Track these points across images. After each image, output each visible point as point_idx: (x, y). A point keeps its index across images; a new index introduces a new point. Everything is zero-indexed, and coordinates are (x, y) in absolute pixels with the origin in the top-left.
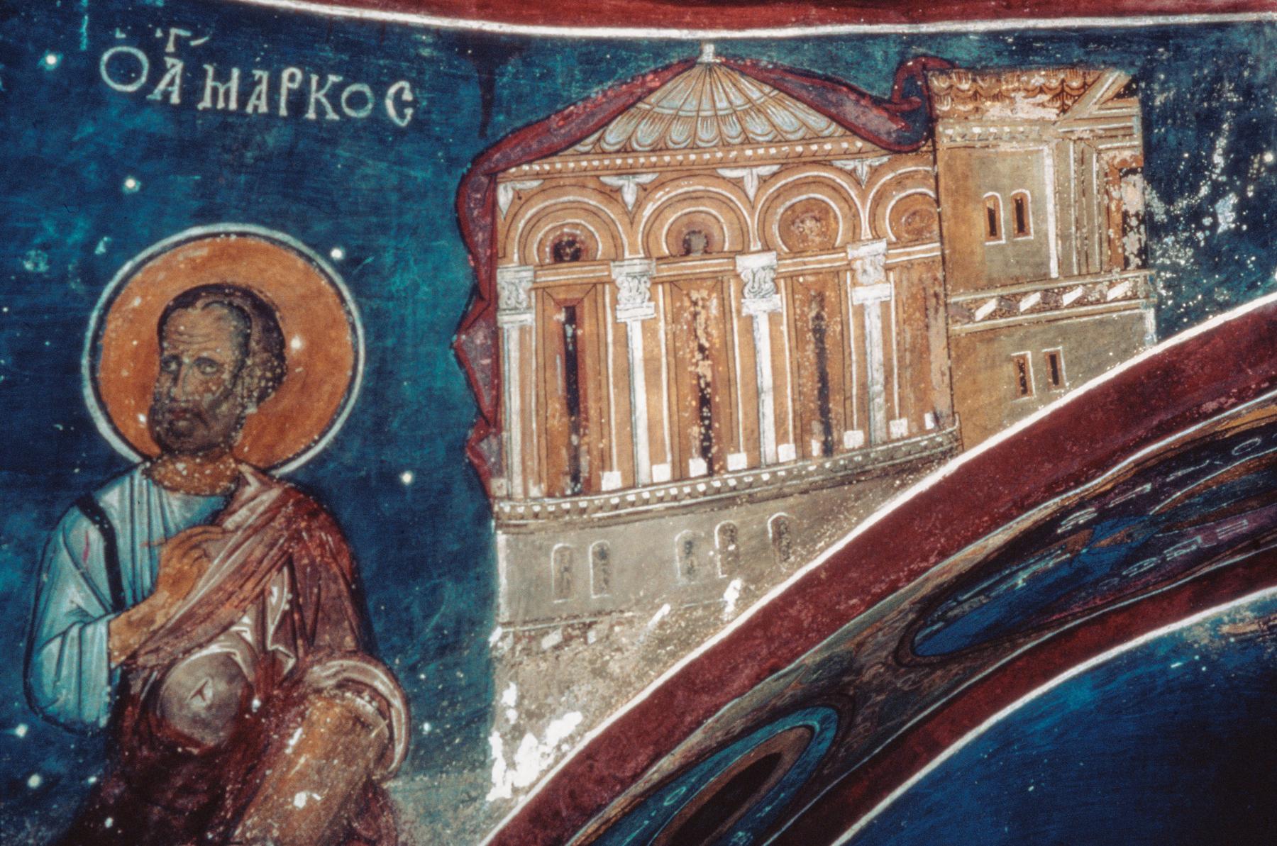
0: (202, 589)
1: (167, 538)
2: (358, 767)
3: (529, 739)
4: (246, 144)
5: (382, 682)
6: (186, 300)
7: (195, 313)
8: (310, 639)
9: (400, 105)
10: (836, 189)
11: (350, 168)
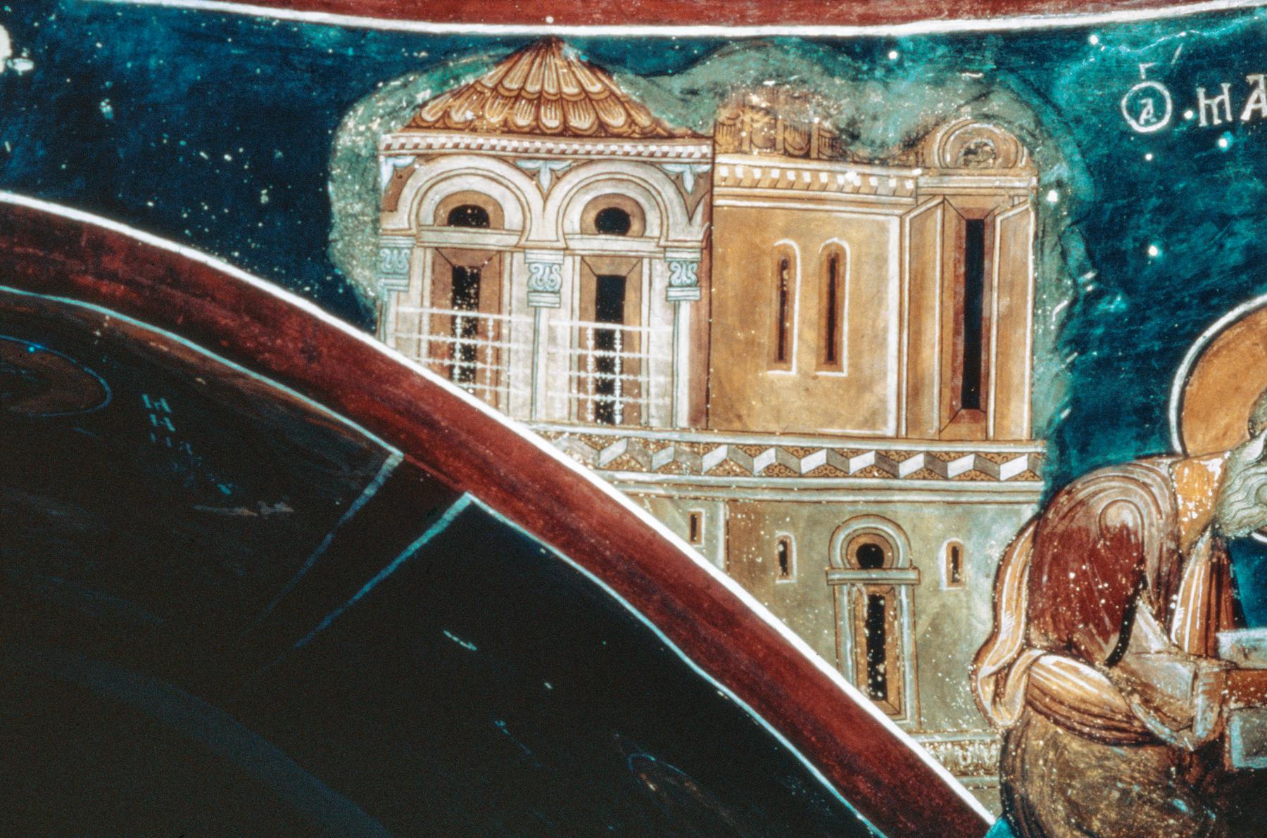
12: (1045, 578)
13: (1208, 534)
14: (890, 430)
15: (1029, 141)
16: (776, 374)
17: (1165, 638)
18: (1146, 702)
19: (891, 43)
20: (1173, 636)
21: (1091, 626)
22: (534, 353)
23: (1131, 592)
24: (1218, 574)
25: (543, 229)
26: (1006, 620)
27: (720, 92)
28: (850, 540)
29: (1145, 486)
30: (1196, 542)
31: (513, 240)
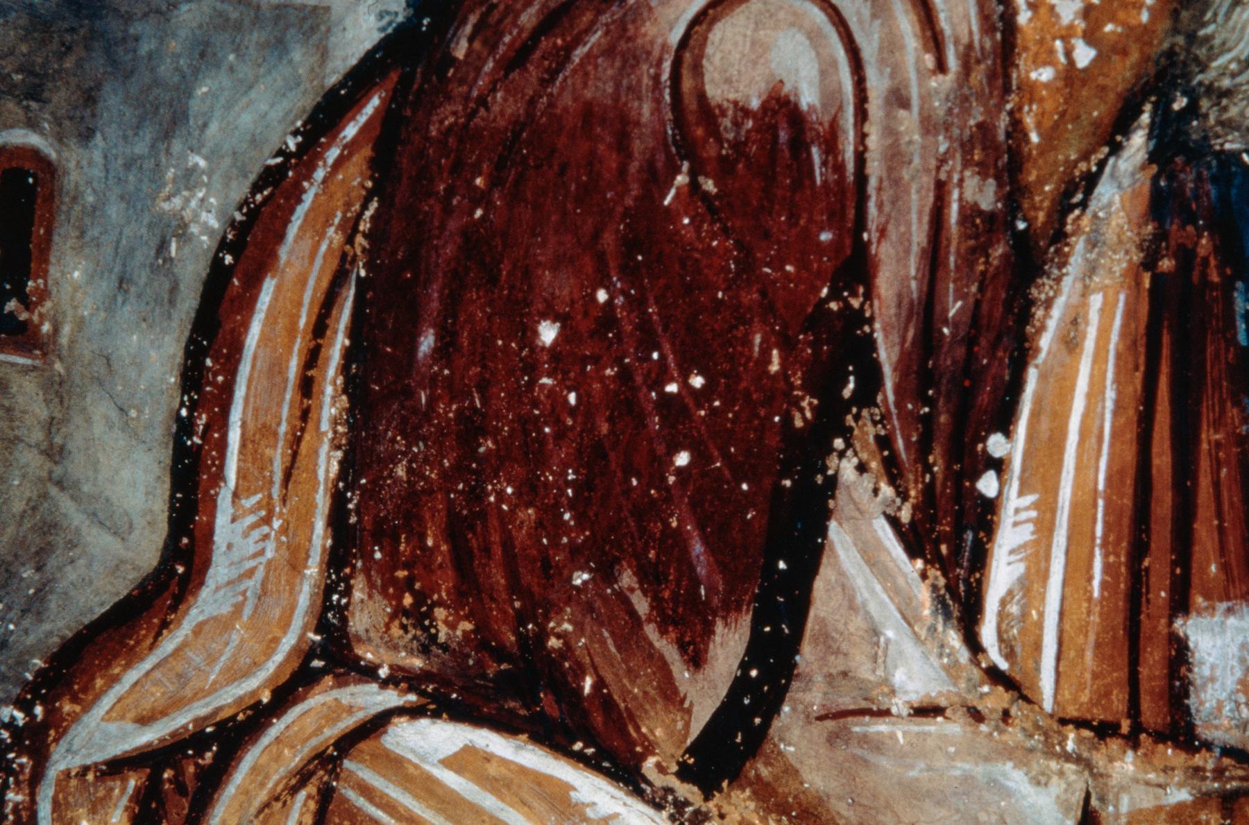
12: (427, 343)
13: (1138, 143)
17: (954, 639)
20: (988, 633)
21: (627, 579)
23: (805, 411)
26: (235, 533)
30: (1091, 181)
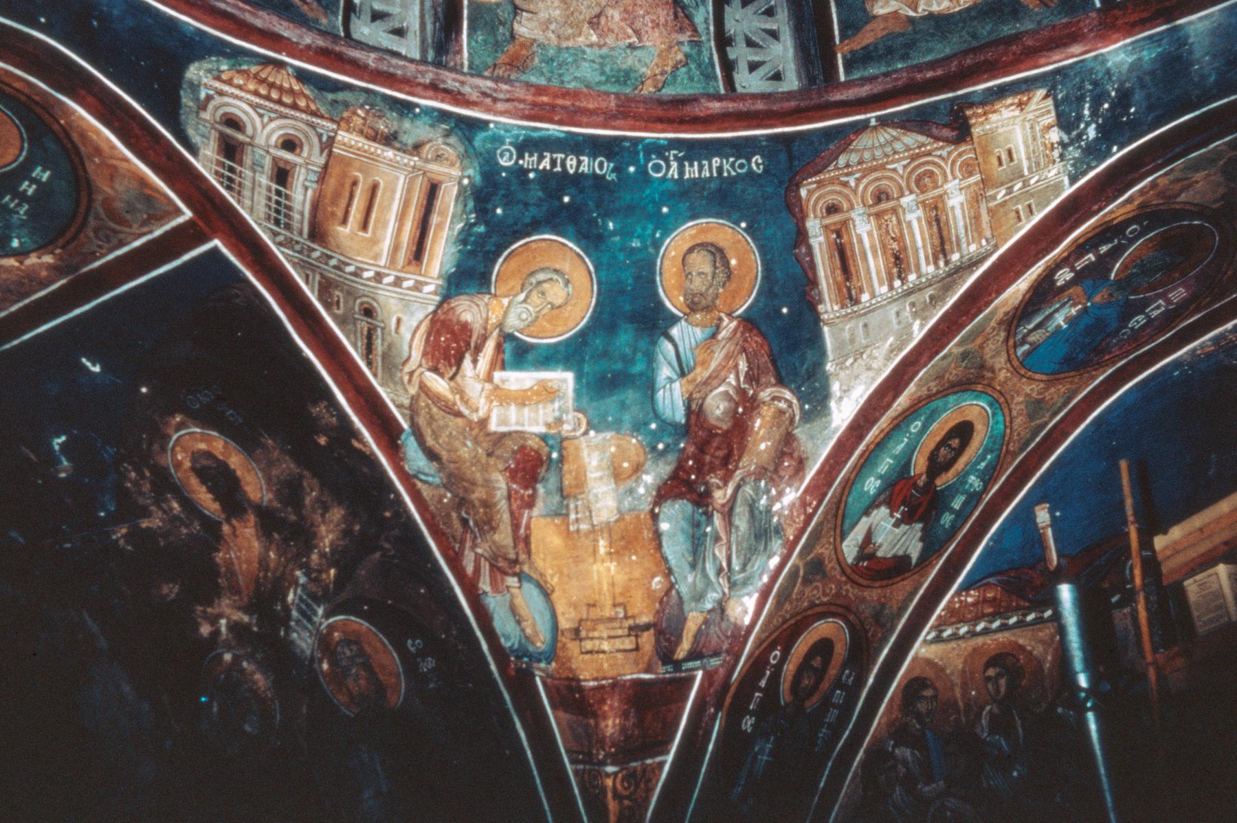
0: (713, 365)
1: (697, 346)
2: (783, 429)
3: (845, 399)
4: (703, 188)
5: (788, 395)
6: (691, 250)
7: (694, 255)
8: (758, 382)
9: (758, 165)
10: (934, 163)
11: (743, 191)
14: (382, 263)
15: (465, 156)
16: (340, 229)
18: (462, 398)
19: (417, 105)
22: (253, 189)
24: (499, 348)
25: (260, 140)
27: (346, 105)
28: (362, 304)
29: (478, 306)
31: (248, 140)
